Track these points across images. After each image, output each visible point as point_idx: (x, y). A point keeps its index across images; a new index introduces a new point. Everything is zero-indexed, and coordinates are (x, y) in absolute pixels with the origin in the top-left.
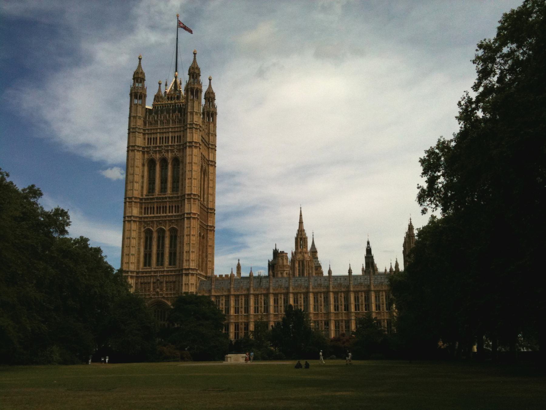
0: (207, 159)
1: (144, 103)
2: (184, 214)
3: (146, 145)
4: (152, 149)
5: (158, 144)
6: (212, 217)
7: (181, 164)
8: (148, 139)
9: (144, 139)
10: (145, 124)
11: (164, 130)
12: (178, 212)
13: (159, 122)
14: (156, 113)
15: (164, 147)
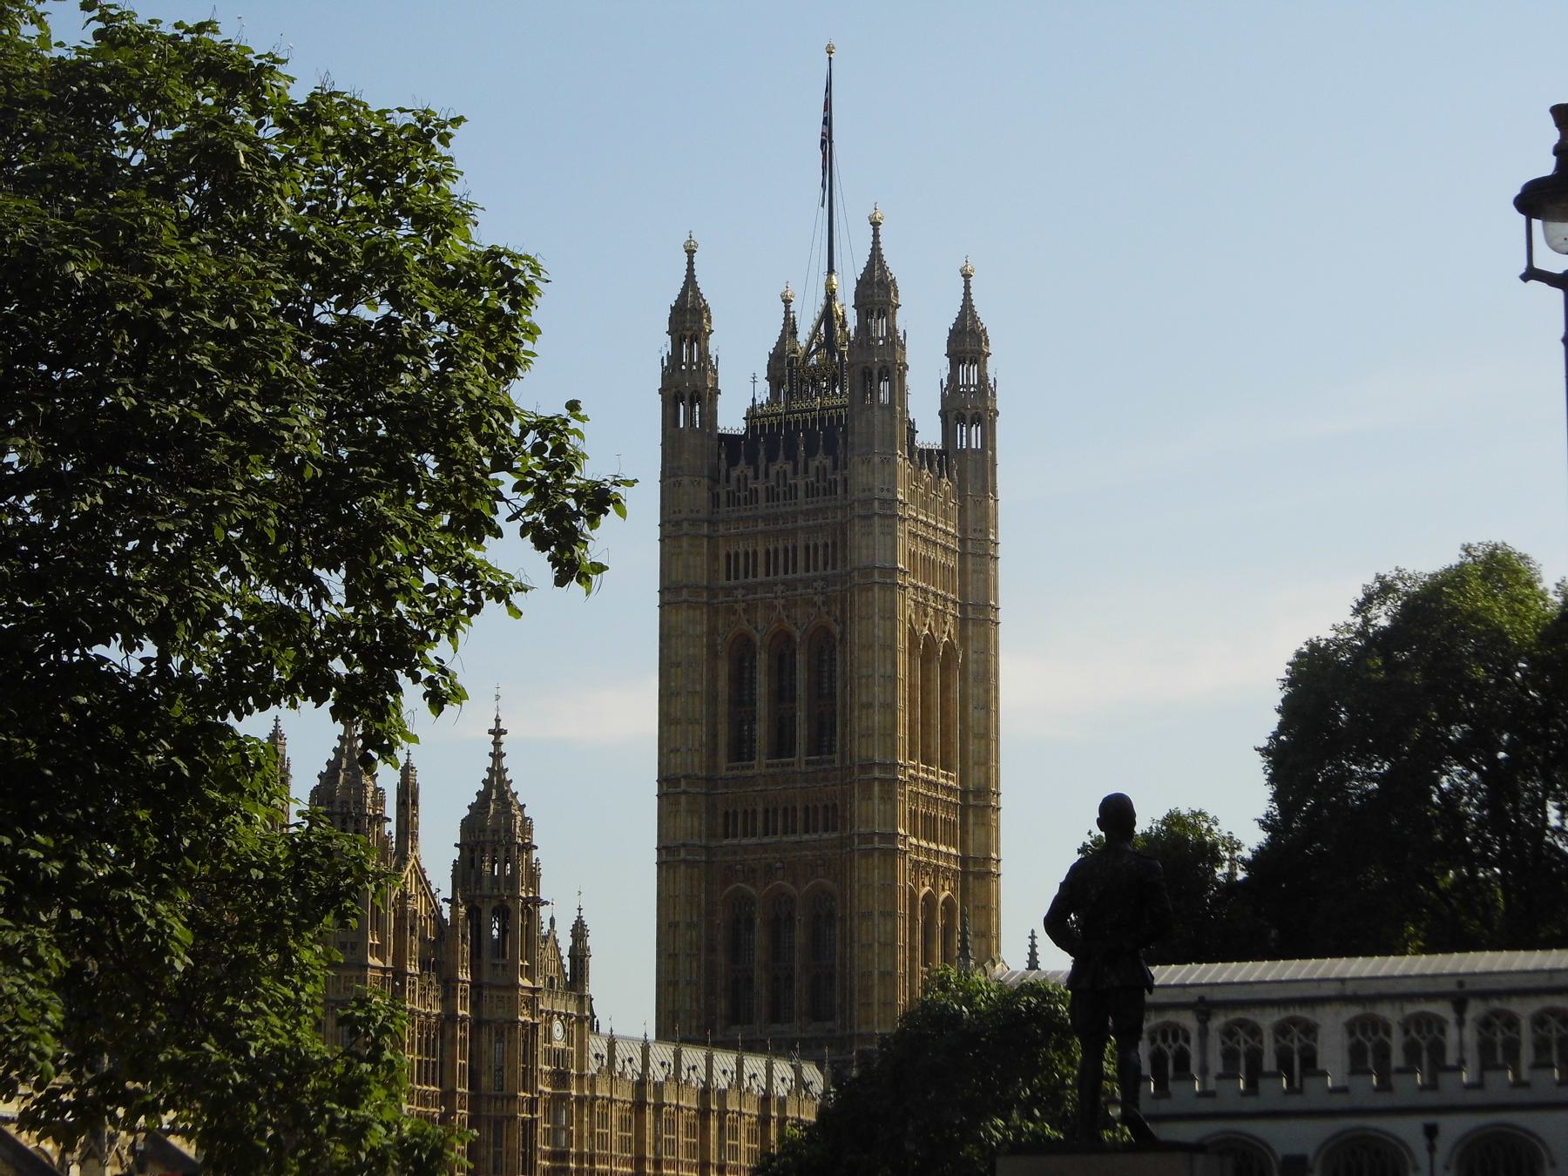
0: (954, 602)
1: (710, 416)
2: (851, 837)
3: (723, 582)
4: (740, 596)
5: (761, 577)
6: (983, 824)
7: (838, 649)
8: (728, 556)
9: (714, 556)
10: (715, 499)
11: (781, 526)
12: (834, 829)
13: (762, 495)
14: (752, 460)
15: (780, 588)
